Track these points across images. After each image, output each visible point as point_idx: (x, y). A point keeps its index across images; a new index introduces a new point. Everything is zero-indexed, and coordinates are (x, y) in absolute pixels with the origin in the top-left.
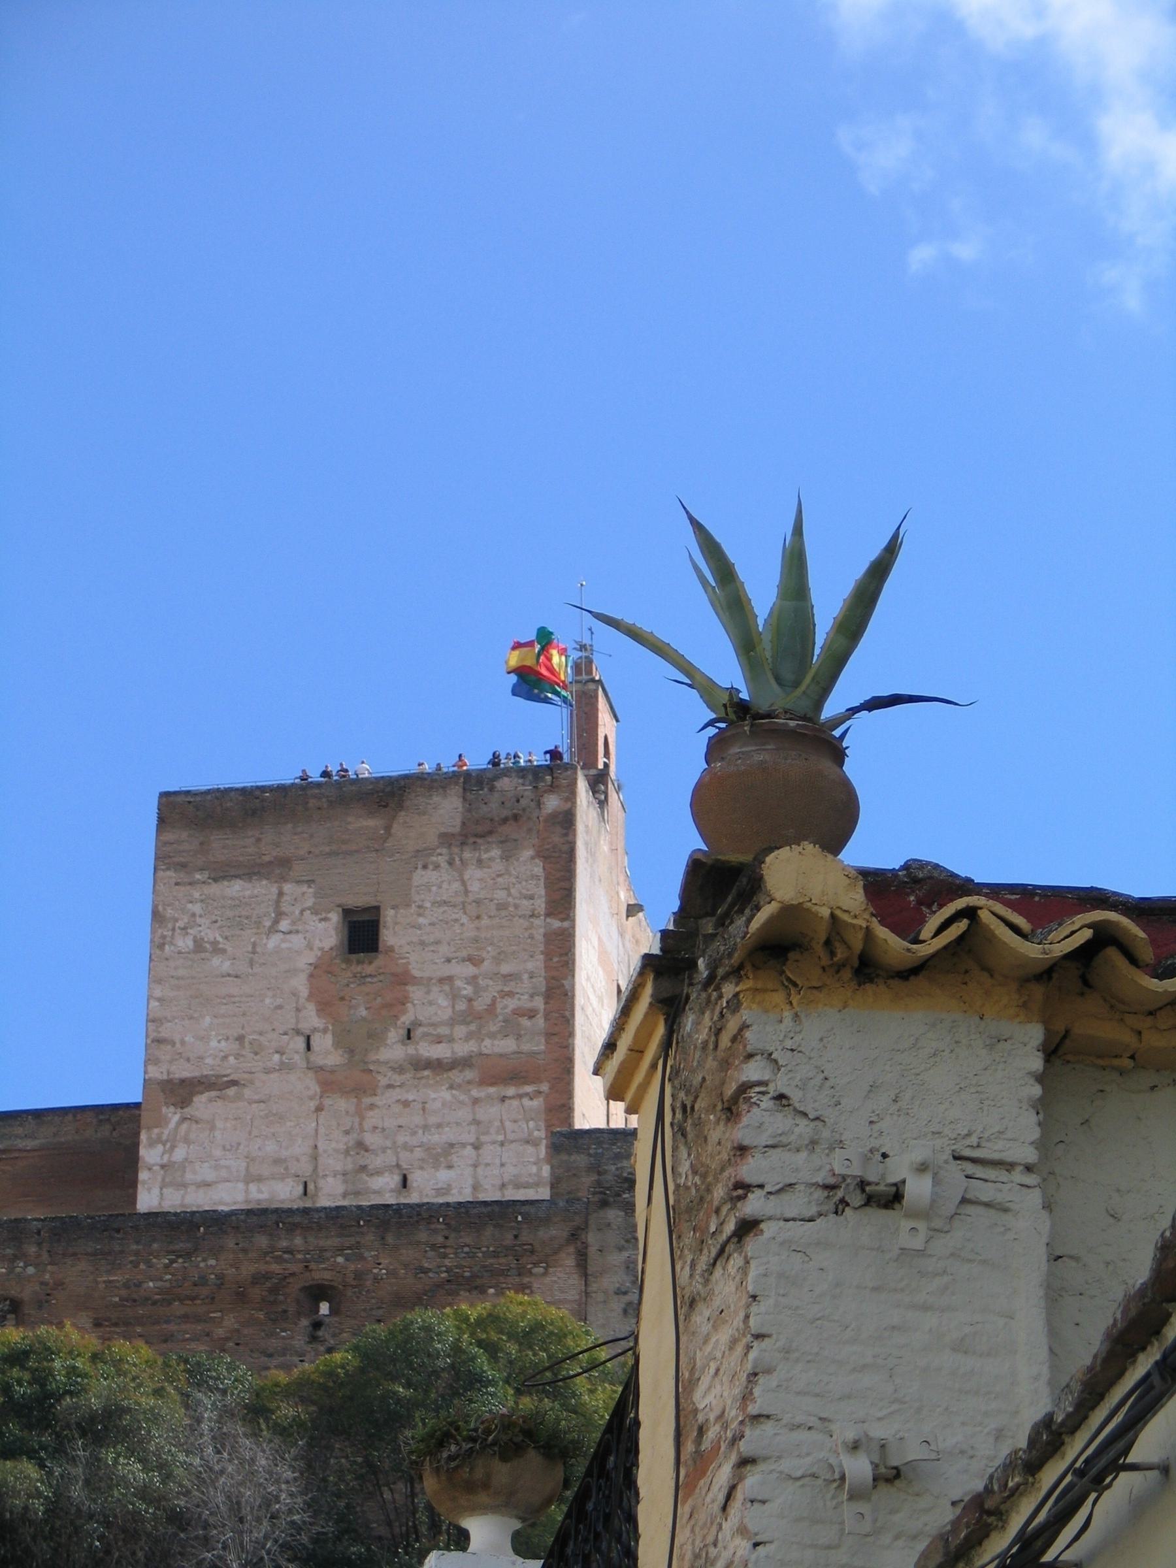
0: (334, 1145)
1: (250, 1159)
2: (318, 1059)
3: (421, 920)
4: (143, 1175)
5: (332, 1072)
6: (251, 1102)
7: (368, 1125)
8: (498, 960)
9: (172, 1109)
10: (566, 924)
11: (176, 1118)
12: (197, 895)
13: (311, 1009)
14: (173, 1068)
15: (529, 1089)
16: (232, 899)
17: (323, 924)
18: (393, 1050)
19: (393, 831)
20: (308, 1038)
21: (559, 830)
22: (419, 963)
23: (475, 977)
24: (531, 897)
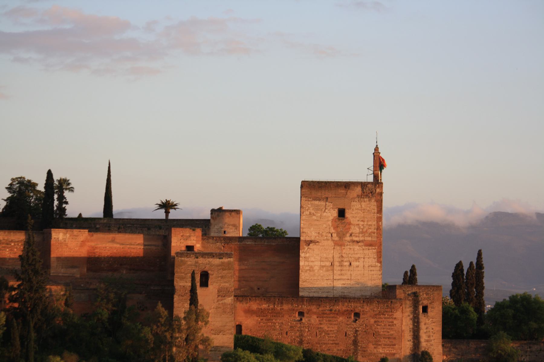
0: (337, 256)
1: (321, 257)
2: (334, 239)
3: (353, 212)
4: (301, 259)
5: (336, 241)
6: (321, 246)
7: (343, 252)
8: (368, 221)
9: (306, 246)
10: (381, 215)
11: (307, 248)
12: (309, 203)
13: (332, 228)
14: (306, 238)
15: (374, 248)
16: (316, 204)
17: (334, 211)
18: (348, 238)
19: (348, 193)
20: (332, 234)
21: (379, 196)
22: (353, 221)
23: (363, 225)
24: (374, 209)
